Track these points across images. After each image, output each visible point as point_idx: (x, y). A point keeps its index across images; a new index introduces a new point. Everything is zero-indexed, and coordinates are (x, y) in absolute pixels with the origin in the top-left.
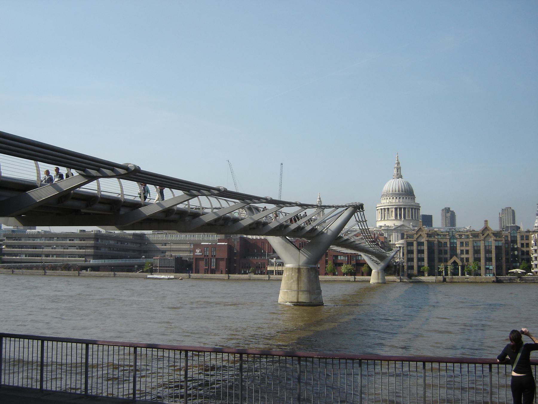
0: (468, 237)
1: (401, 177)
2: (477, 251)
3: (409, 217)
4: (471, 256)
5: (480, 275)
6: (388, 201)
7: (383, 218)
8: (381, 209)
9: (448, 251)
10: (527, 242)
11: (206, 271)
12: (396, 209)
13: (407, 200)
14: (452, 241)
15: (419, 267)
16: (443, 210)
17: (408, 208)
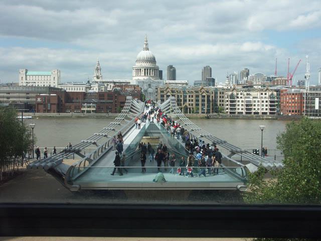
2: (197, 101)
3: (152, 74)
4: (194, 103)
7: (137, 75)
11: (45, 111)
12: (145, 69)
16: (168, 67)
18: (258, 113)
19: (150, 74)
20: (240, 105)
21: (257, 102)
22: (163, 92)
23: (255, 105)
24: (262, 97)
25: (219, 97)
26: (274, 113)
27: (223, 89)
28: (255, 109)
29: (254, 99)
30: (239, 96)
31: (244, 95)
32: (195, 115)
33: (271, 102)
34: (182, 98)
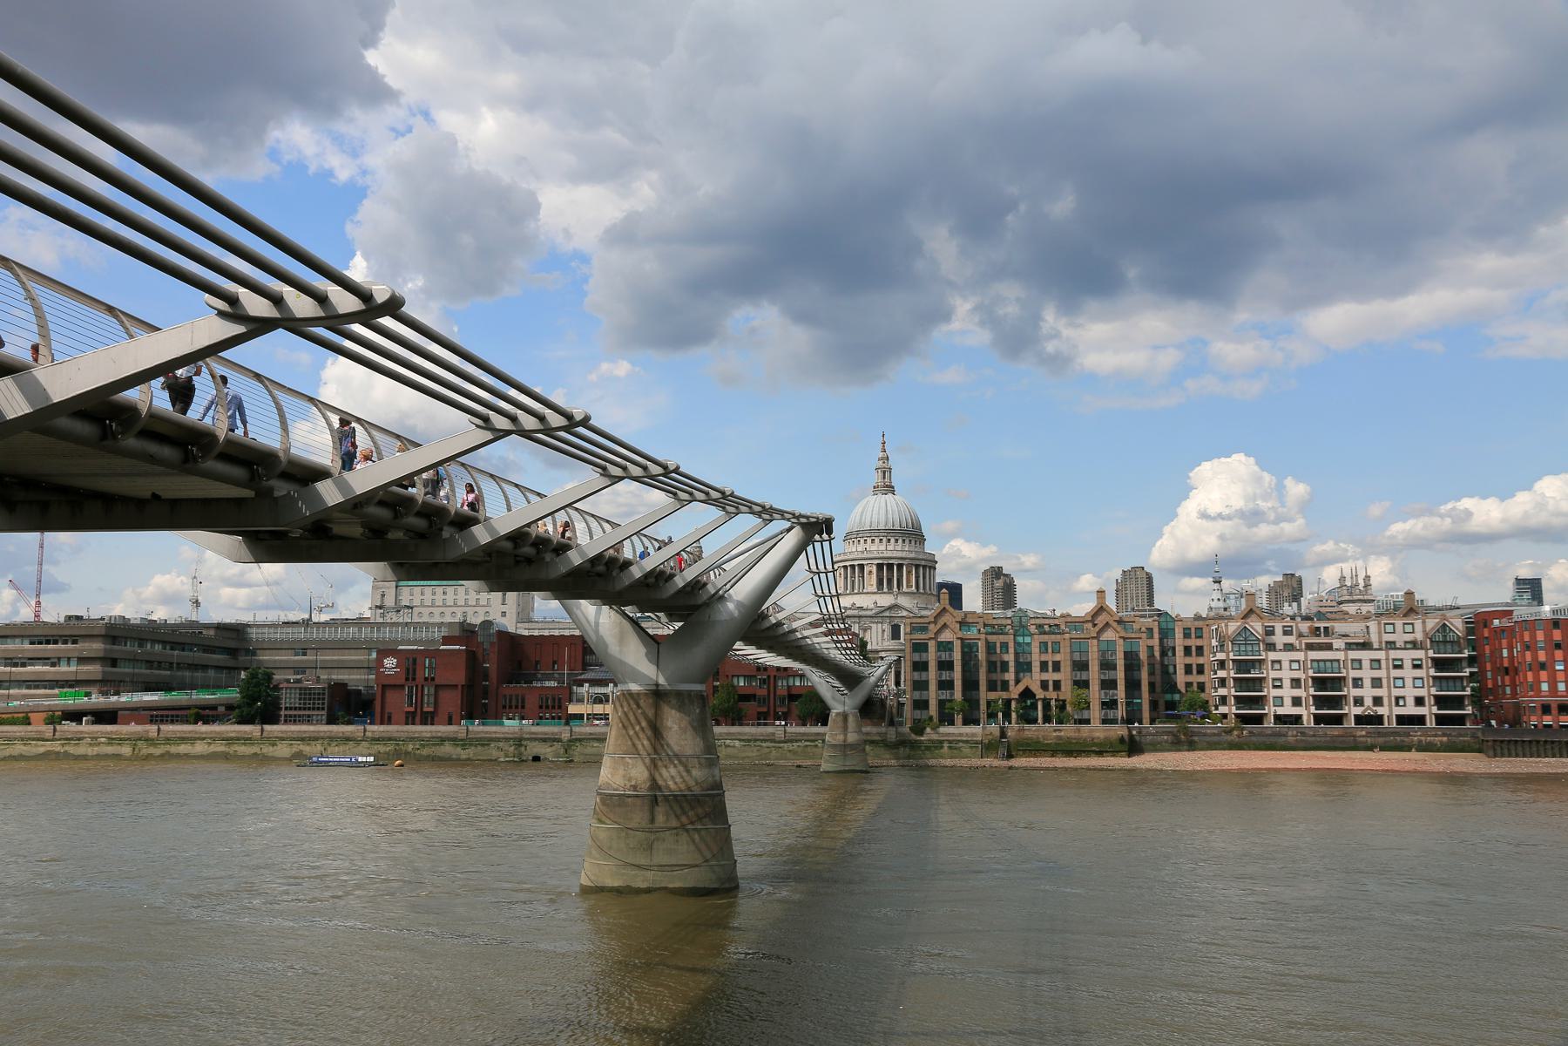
0: (1055, 629)
3: (909, 586)
4: (1065, 676)
5: (1087, 722)
9: (1012, 664)
10: (1199, 642)
11: (410, 719)
12: (880, 567)
14: (1020, 639)
15: (941, 703)
17: (909, 566)
18: (1378, 719)
20: (1287, 683)
21: (1366, 664)
22: (924, 629)
23: (1357, 683)
24: (1391, 645)
25: (1180, 651)
26: (1460, 720)
27: (1198, 618)
28: (1359, 701)
29: (1354, 654)
30: (1279, 639)
31: (1300, 635)
32: (1068, 730)
34: (1010, 658)
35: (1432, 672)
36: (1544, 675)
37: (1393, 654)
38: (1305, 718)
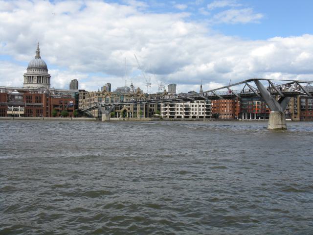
1: (40, 58)
4: (131, 107)
6: (32, 72)
8: (28, 77)
12: (38, 77)
13: (43, 72)
18: (195, 117)
19: (43, 82)
20: (179, 109)
23: (193, 110)
26: (209, 117)
28: (193, 113)
33: (206, 106)
35: (206, 108)
36: (225, 109)
37: (199, 104)
38: (182, 116)
